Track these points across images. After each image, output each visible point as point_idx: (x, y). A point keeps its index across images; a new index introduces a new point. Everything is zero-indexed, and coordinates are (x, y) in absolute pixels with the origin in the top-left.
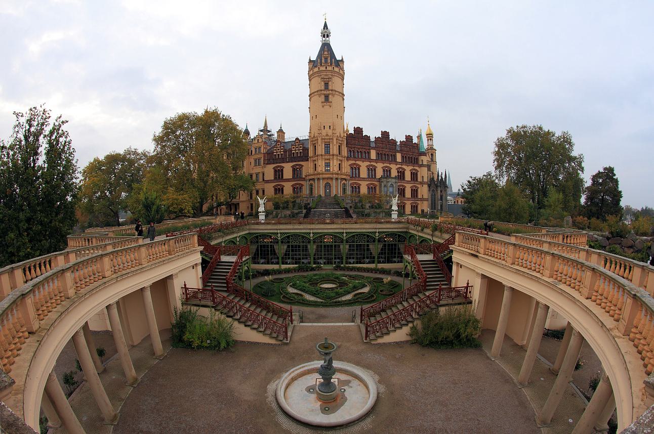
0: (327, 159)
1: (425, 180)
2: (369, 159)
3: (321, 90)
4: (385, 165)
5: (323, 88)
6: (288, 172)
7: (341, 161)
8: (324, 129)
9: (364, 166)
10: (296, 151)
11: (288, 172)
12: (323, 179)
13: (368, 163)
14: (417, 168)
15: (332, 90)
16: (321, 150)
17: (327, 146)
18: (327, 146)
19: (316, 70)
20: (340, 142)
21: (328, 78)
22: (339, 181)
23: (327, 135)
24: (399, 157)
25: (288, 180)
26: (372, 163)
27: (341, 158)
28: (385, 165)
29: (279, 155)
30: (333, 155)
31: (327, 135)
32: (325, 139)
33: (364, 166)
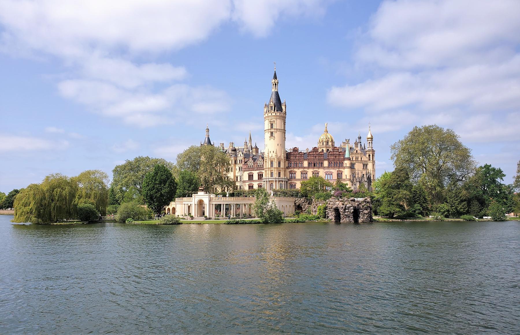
1: (348, 177)
3: (269, 129)
5: (270, 128)
6: (256, 177)
8: (270, 153)
10: (260, 164)
11: (256, 177)
12: (269, 181)
14: (342, 170)
15: (275, 129)
17: (272, 163)
18: (272, 163)
21: (273, 121)
22: (277, 182)
23: (272, 157)
24: (326, 163)
25: (255, 181)
29: (251, 166)
31: (272, 157)
32: (271, 159)
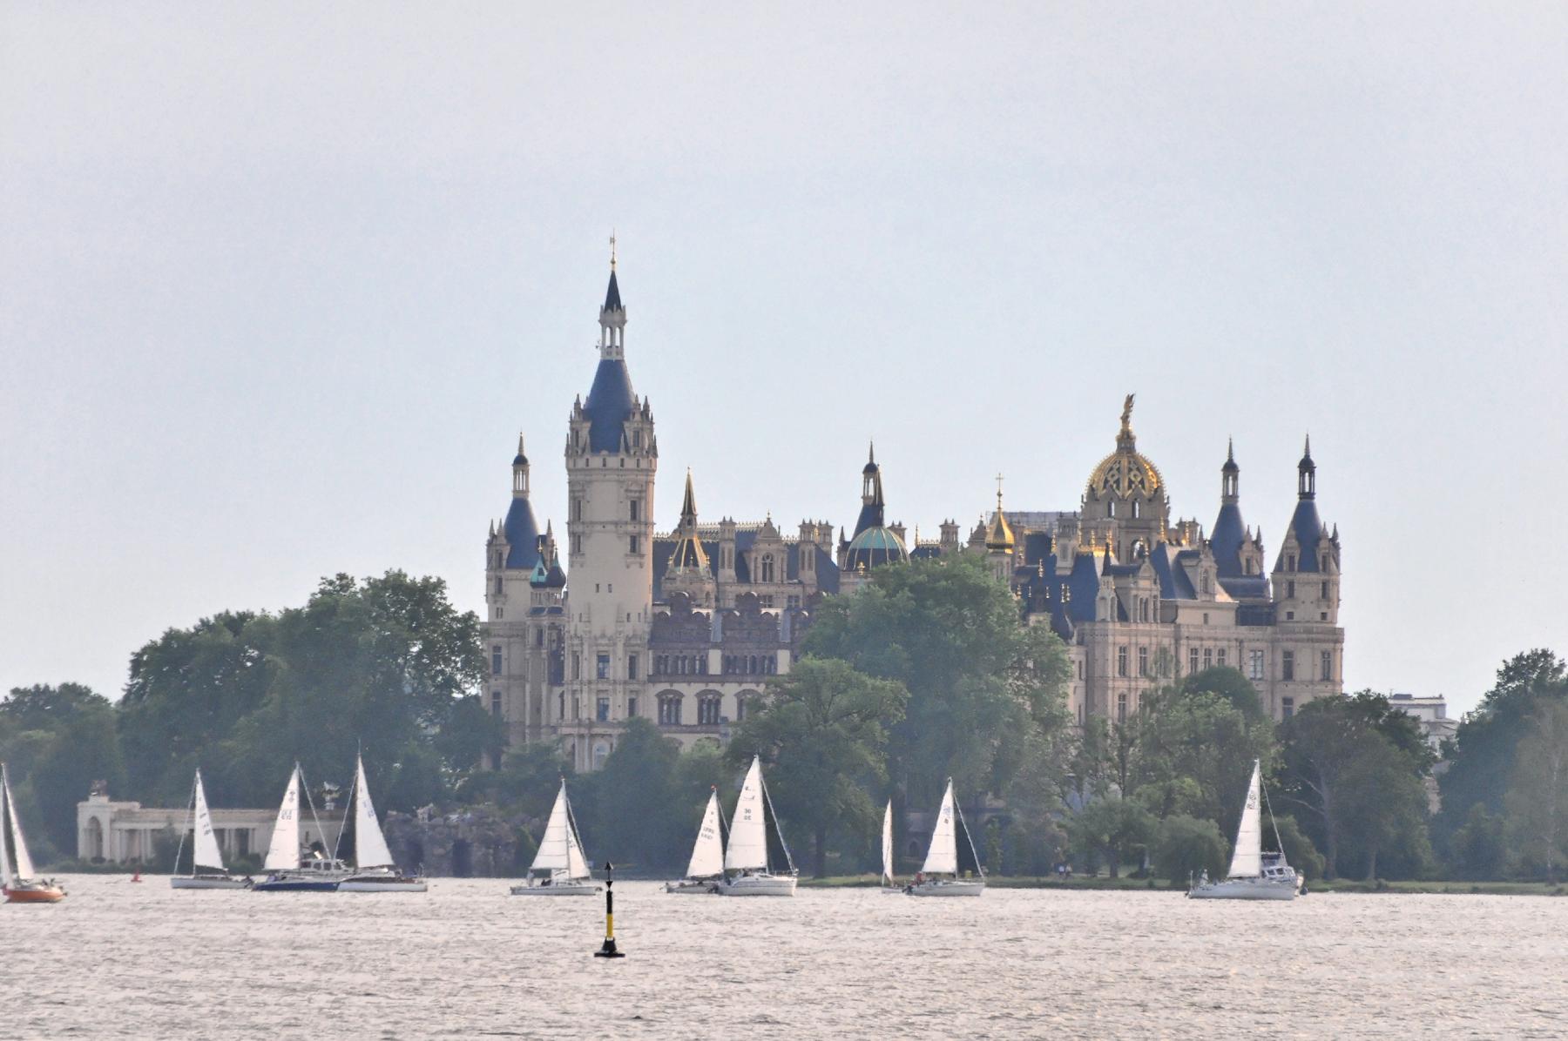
0: (602, 691)
2: (703, 674)
4: (745, 686)
7: (637, 692)
9: (690, 693)
13: (700, 687)
16: (589, 668)
19: (581, 463)
20: (636, 648)
23: (603, 636)
26: (712, 686)
27: (635, 687)
28: (745, 686)
30: (615, 682)
31: (603, 636)
33: (690, 693)
